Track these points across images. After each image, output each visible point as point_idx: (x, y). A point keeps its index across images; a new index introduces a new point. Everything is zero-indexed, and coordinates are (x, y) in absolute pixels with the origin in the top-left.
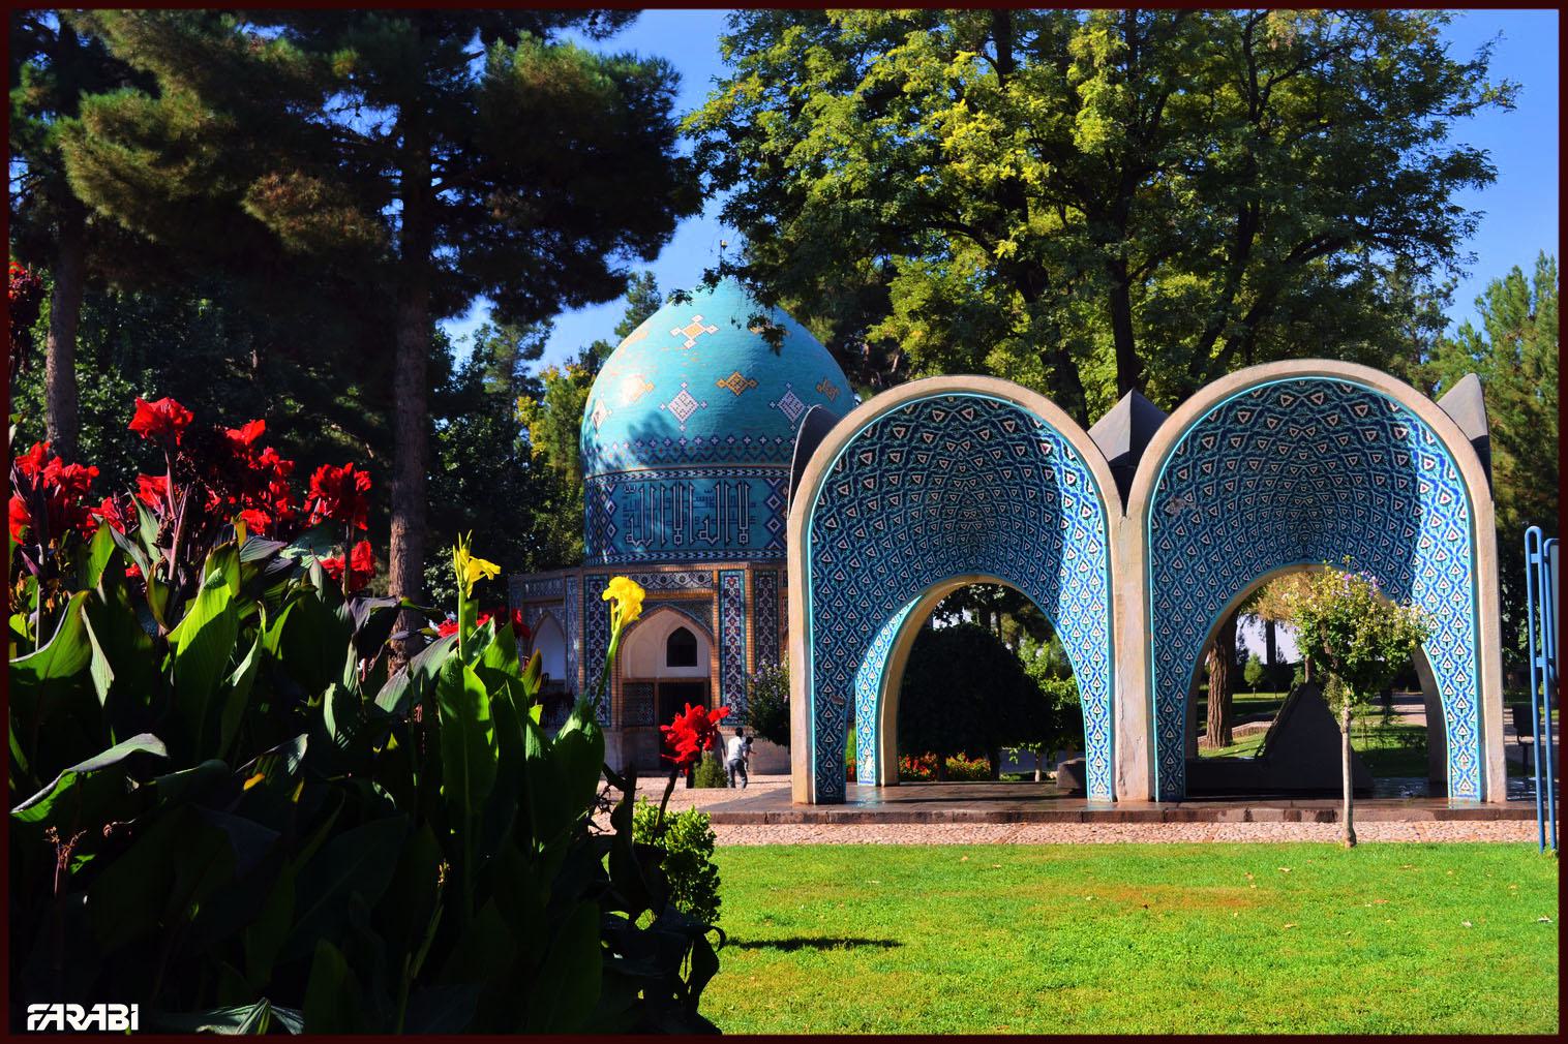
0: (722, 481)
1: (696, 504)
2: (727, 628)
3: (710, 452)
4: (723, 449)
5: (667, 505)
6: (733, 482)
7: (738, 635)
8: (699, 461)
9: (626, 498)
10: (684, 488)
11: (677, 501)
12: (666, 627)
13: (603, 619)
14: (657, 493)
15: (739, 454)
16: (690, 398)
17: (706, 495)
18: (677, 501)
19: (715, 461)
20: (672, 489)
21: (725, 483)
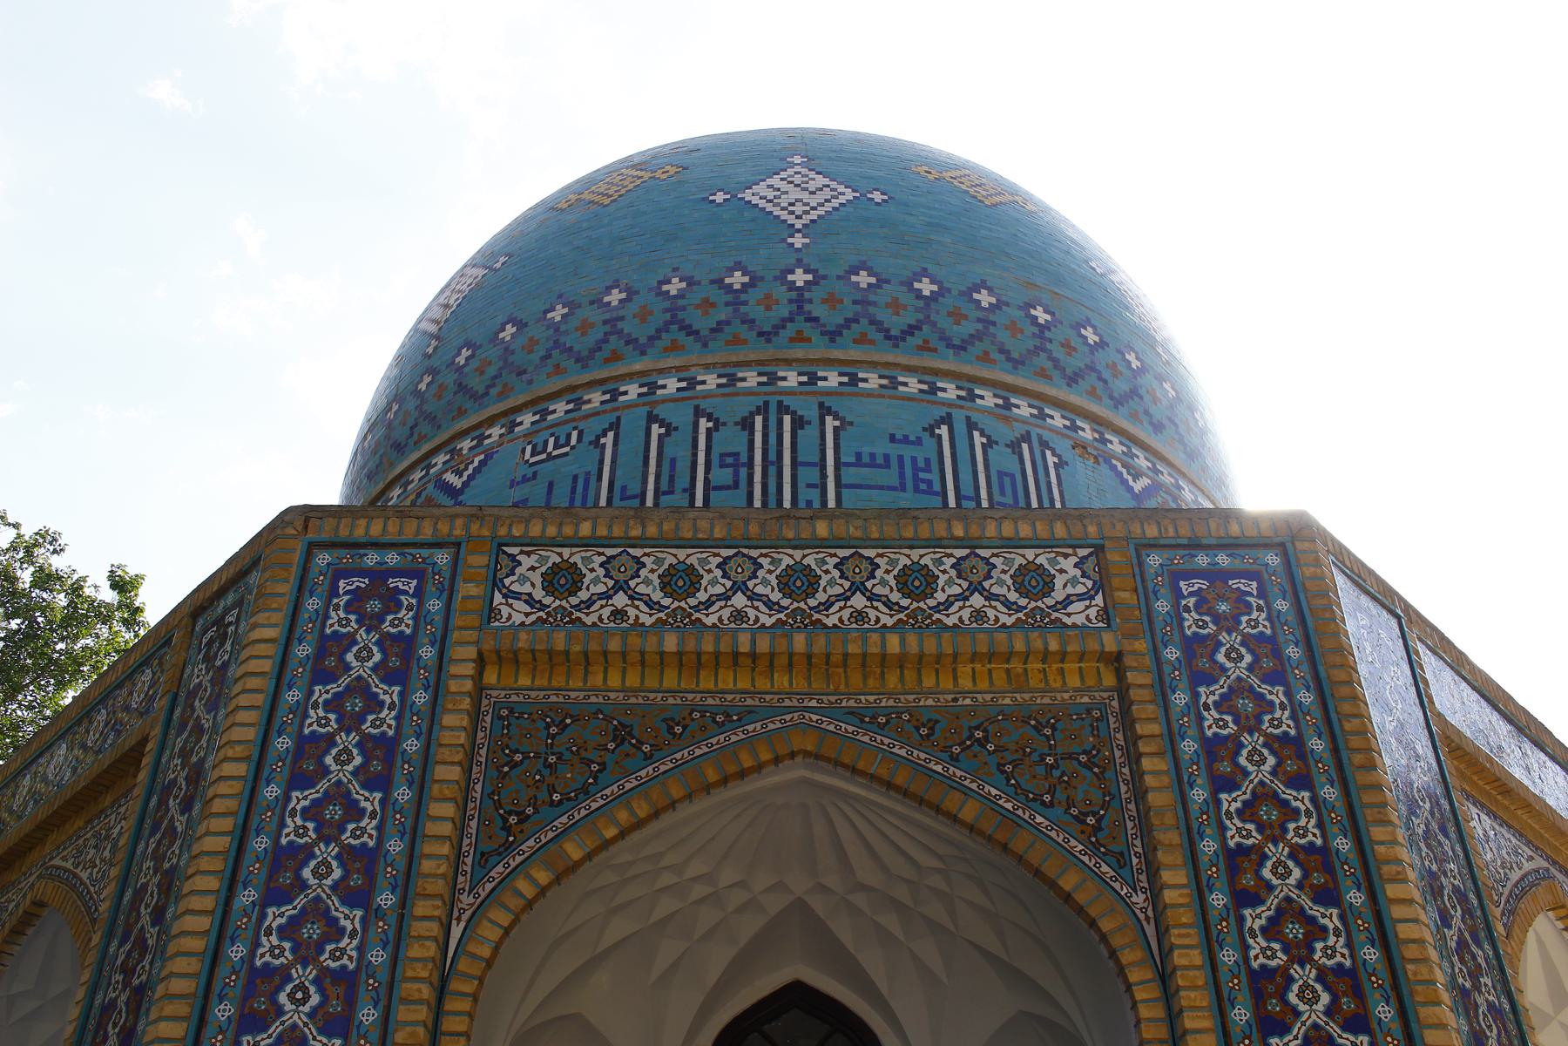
0: (959, 416)
1: (849, 475)
2: (1236, 858)
3: (909, 318)
4: (957, 316)
5: (722, 476)
6: (1004, 433)
7: (1327, 896)
8: (862, 340)
9: (525, 479)
10: (798, 423)
11: (772, 463)
12: (718, 960)
13: (379, 782)
14: (681, 438)
15: (1017, 348)
16: (821, 180)
17: (894, 450)
18: (772, 463)
19: (925, 347)
20: (747, 424)
21: (971, 426)
